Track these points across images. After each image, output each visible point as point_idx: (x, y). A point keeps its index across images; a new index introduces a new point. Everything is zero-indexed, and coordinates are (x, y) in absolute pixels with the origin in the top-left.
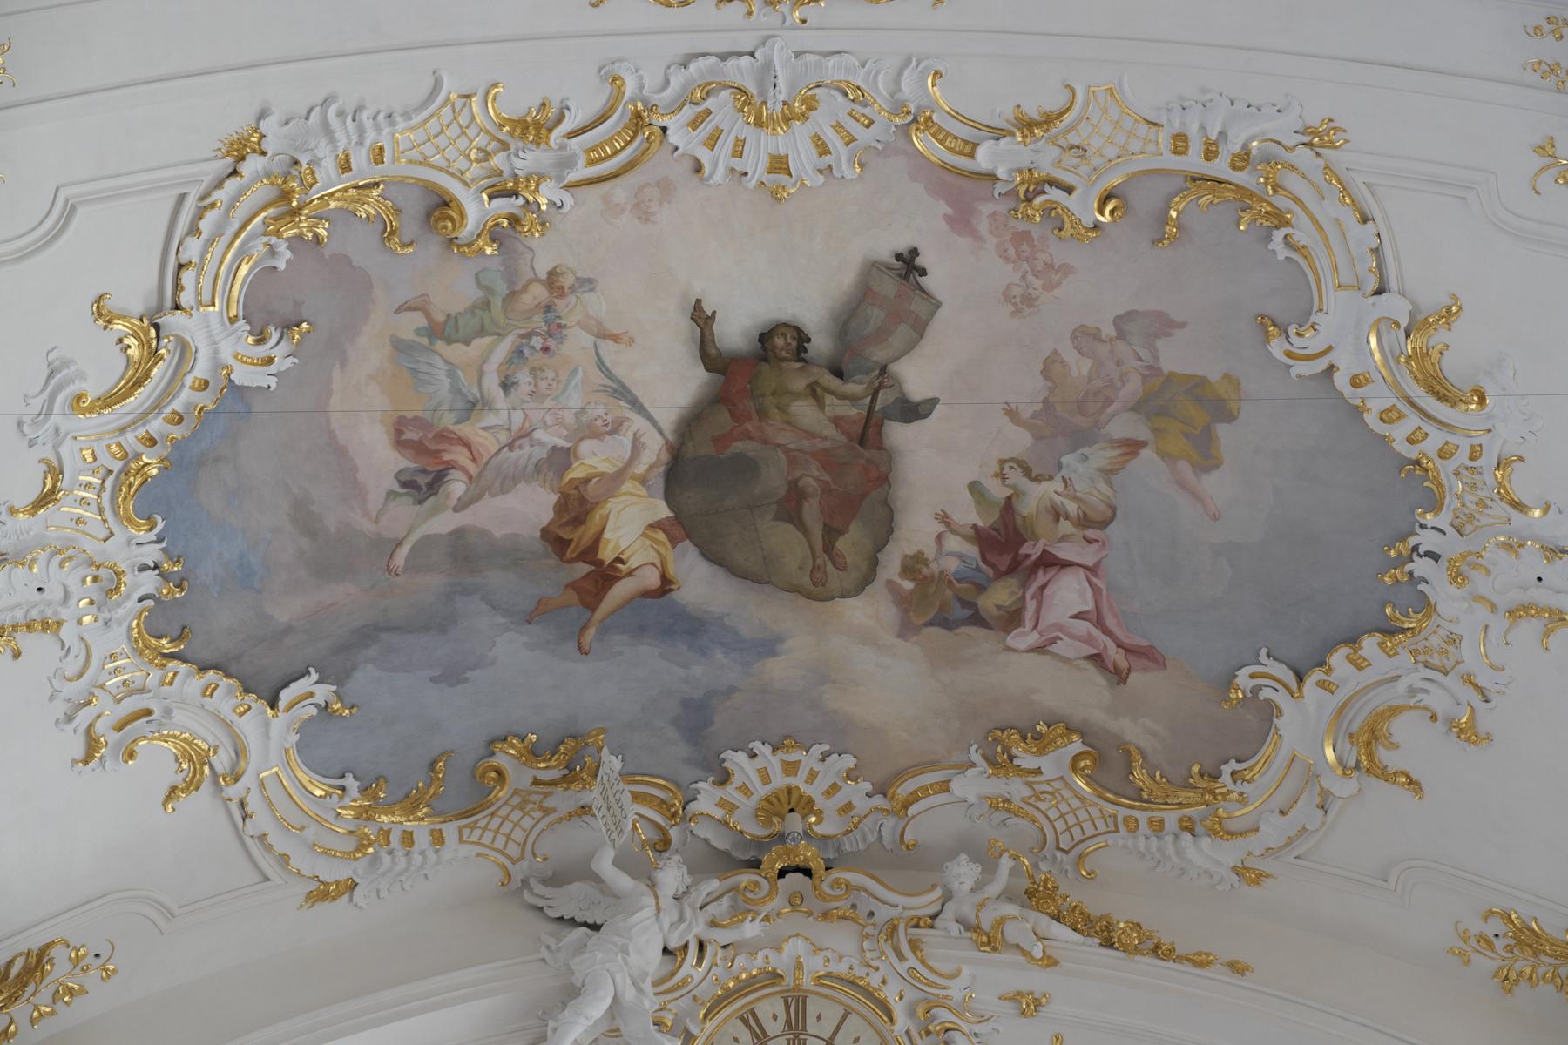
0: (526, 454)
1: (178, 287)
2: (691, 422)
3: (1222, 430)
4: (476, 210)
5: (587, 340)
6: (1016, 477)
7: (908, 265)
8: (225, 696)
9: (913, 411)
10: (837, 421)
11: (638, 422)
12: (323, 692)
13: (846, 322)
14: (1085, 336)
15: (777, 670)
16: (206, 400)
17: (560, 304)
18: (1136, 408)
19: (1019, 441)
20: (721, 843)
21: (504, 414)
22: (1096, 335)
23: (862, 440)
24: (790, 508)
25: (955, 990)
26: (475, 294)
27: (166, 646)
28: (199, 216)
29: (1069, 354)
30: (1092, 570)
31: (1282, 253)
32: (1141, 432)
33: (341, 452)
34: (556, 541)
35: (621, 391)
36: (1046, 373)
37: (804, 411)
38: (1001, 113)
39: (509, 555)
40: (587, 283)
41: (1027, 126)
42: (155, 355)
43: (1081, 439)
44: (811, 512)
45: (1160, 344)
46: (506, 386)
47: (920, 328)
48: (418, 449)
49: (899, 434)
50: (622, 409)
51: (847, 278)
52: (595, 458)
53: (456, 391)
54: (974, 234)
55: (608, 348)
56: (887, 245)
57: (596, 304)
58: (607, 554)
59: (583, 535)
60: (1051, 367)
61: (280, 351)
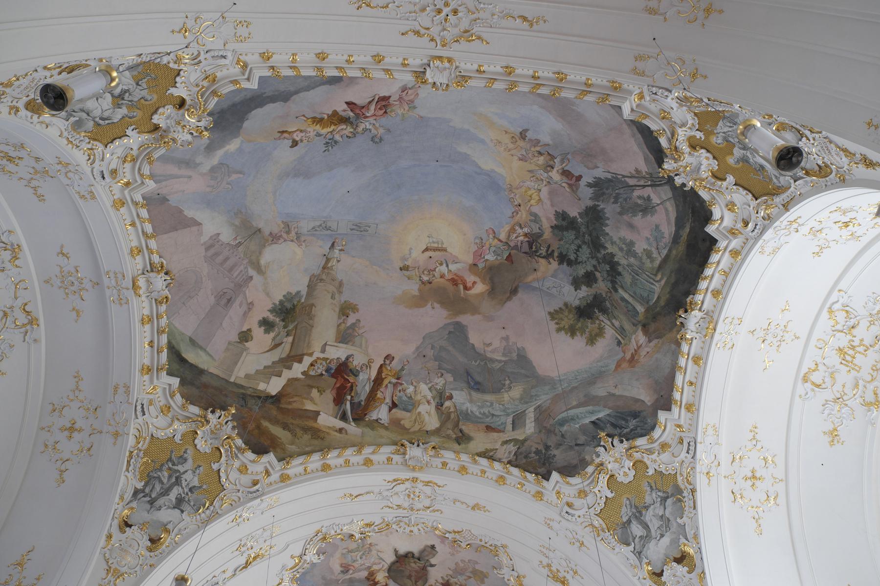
0: (363, 567)
1: (305, 552)
2: (393, 563)
3: (486, 579)
4: (358, 536)
5: (376, 552)
6: (449, 577)
7: (433, 547)
9: (432, 566)
10: (418, 566)
11: (384, 563)
13: (423, 551)
14: (463, 561)
16: (308, 566)
17: (371, 547)
18: (471, 572)
19: (451, 573)
22: (465, 561)
23: (423, 569)
24: (410, 577)
26: (356, 546)
28: (310, 542)
29: (460, 563)
31: (497, 560)
32: (472, 576)
33: (331, 568)
34: (367, 579)
35: (381, 559)
36: (456, 564)
37: (413, 565)
38: (451, 530)
39: (360, 581)
40: (377, 545)
41: (455, 532)
42: (300, 561)
43: (460, 574)
44: (413, 578)
45: (476, 565)
46: (361, 558)
47: (434, 555)
48: (345, 567)
49: (429, 568)
50: (381, 561)
51: (422, 547)
52: (375, 567)
53: (352, 559)
54: (445, 544)
55: (379, 554)
56: (430, 543)
57: (378, 547)
58: (376, 580)
59: (373, 578)
60: (456, 564)
61: (322, 557)
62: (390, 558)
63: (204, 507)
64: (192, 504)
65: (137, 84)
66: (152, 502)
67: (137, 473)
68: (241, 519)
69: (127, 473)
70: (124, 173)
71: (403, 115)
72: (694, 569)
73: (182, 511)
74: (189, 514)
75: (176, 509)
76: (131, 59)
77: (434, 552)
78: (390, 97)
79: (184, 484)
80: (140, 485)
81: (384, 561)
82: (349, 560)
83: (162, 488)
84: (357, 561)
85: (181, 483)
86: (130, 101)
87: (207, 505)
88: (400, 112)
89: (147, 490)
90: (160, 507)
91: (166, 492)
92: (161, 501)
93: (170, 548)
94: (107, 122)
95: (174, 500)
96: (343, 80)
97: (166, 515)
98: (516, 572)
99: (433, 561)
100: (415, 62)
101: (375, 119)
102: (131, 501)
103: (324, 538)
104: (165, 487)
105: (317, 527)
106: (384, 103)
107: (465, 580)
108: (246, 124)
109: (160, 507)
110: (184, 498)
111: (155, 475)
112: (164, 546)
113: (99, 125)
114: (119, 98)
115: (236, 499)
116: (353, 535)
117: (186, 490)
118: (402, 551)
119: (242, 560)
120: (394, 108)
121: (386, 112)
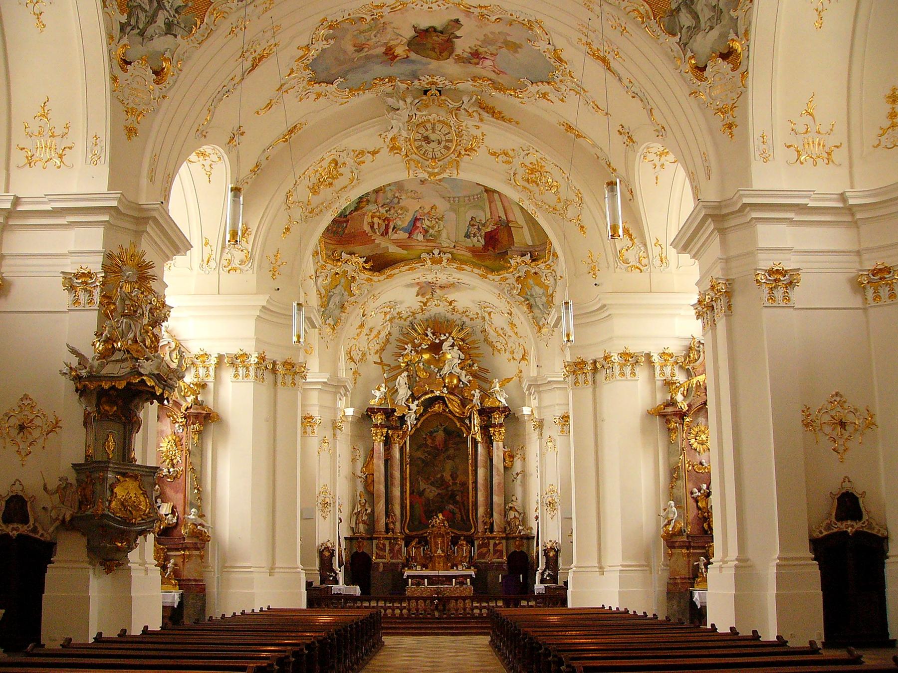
1: (312, 41)
3: (519, 49)
4: (369, 18)
7: (457, 21)
8: (324, 85)
9: (458, 37)
11: (401, 38)
12: (342, 79)
14: (491, 33)
15: (430, 67)
19: (479, 43)
20: (420, 88)
21: (374, 39)
23: (447, 41)
24: (433, 49)
25: (464, 124)
27: (313, 83)
29: (489, 34)
30: (493, 61)
34: (386, 53)
35: (398, 34)
37: (435, 38)
39: (377, 56)
40: (392, 23)
41: (481, 7)
43: (490, 44)
49: (454, 40)
52: (392, 43)
53: (365, 39)
57: (392, 25)
58: (395, 54)
59: (392, 52)
61: (332, 42)
62: (411, 34)
63: (196, 27)
64: (183, 25)
66: (142, 34)
67: (116, 7)
68: (238, 29)
69: (106, 9)
72: (738, 67)
73: (175, 36)
74: (182, 38)
75: (168, 35)
77: (458, 25)
79: (168, 6)
80: (124, 19)
81: (401, 36)
82: (362, 39)
83: (146, 16)
84: (372, 39)
85: (164, 5)
87: (199, 23)
89: (133, 22)
90: (152, 36)
91: (152, 20)
92: (150, 30)
93: (174, 78)
95: (163, 26)
97: (161, 43)
98: (553, 45)
99: (458, 33)
102: (121, 38)
103: (331, 27)
104: (150, 14)
105: (322, 17)
107: (497, 49)
109: (152, 36)
110: (172, 21)
111: (135, 4)
112: (169, 75)
115: (227, 10)
116: (363, 18)
117: (172, 12)
118: (424, 24)
119: (248, 64)
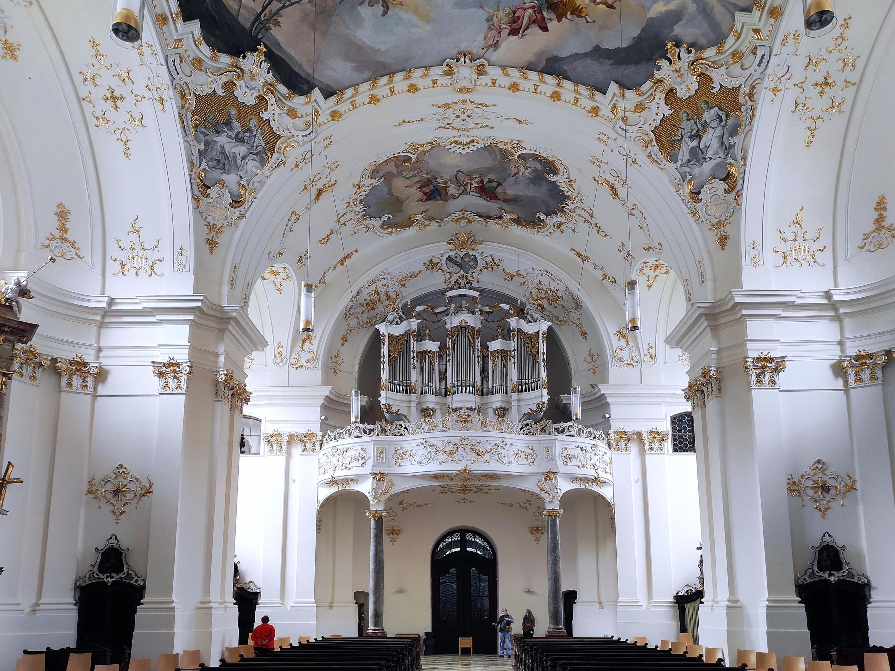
65: (682, 138)
70: (750, 42)
71: (498, 11)
76: (671, 166)
78: (508, 35)
86: (696, 123)
88: (501, 14)
94: (721, 113)
96: (546, 59)
100: (485, 80)
101: (525, 4)
106: (515, 26)
108: (636, 32)
113: (727, 116)
114: (697, 136)
120: (506, 19)
121: (514, 13)
